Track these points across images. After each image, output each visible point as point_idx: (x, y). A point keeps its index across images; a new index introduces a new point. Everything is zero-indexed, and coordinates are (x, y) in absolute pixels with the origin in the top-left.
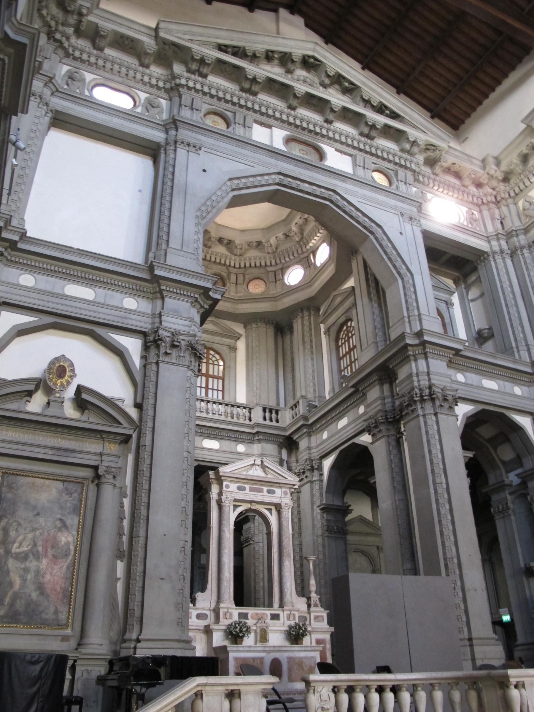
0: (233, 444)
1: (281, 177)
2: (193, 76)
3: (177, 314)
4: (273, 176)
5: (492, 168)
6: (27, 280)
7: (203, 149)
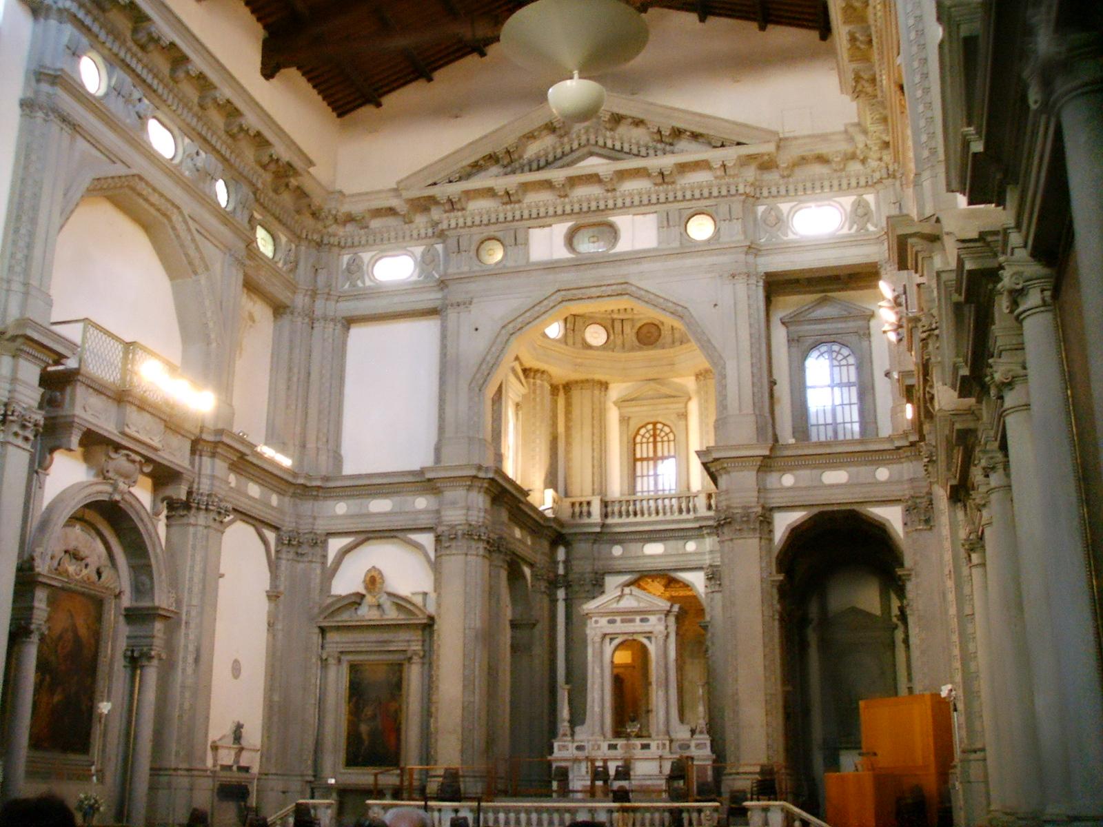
0: (681, 543)
1: (563, 293)
2: (452, 214)
3: (453, 503)
4: (553, 298)
5: (860, 140)
6: (341, 508)
7: (475, 300)
